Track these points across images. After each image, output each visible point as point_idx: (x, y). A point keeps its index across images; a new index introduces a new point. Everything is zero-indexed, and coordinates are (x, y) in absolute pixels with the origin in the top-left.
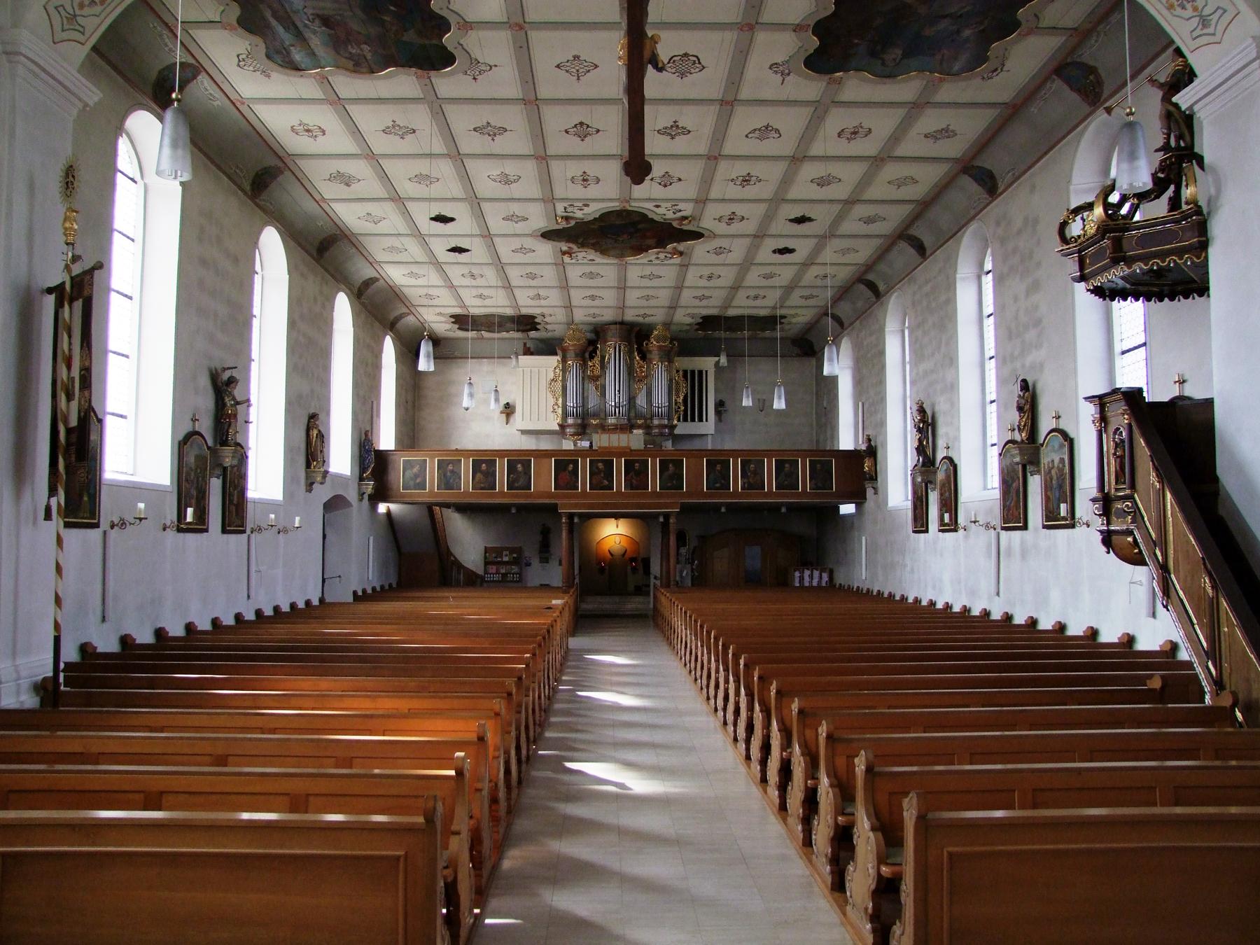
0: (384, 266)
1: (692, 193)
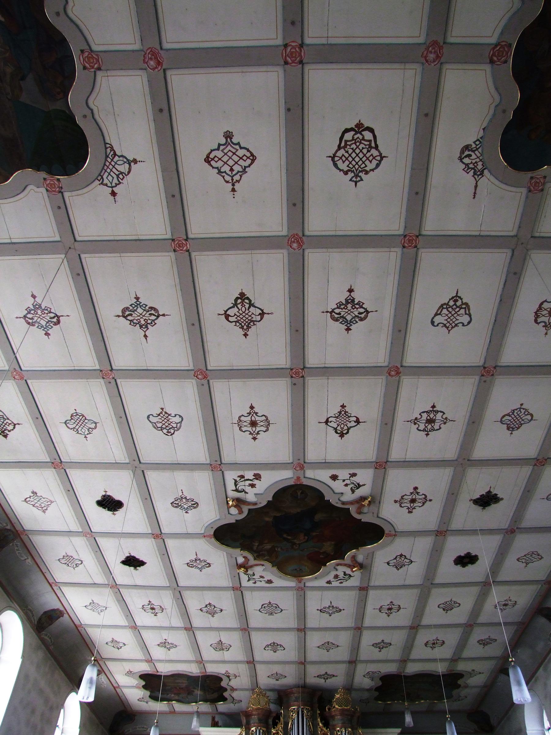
0: (65, 589)
1: (369, 453)
